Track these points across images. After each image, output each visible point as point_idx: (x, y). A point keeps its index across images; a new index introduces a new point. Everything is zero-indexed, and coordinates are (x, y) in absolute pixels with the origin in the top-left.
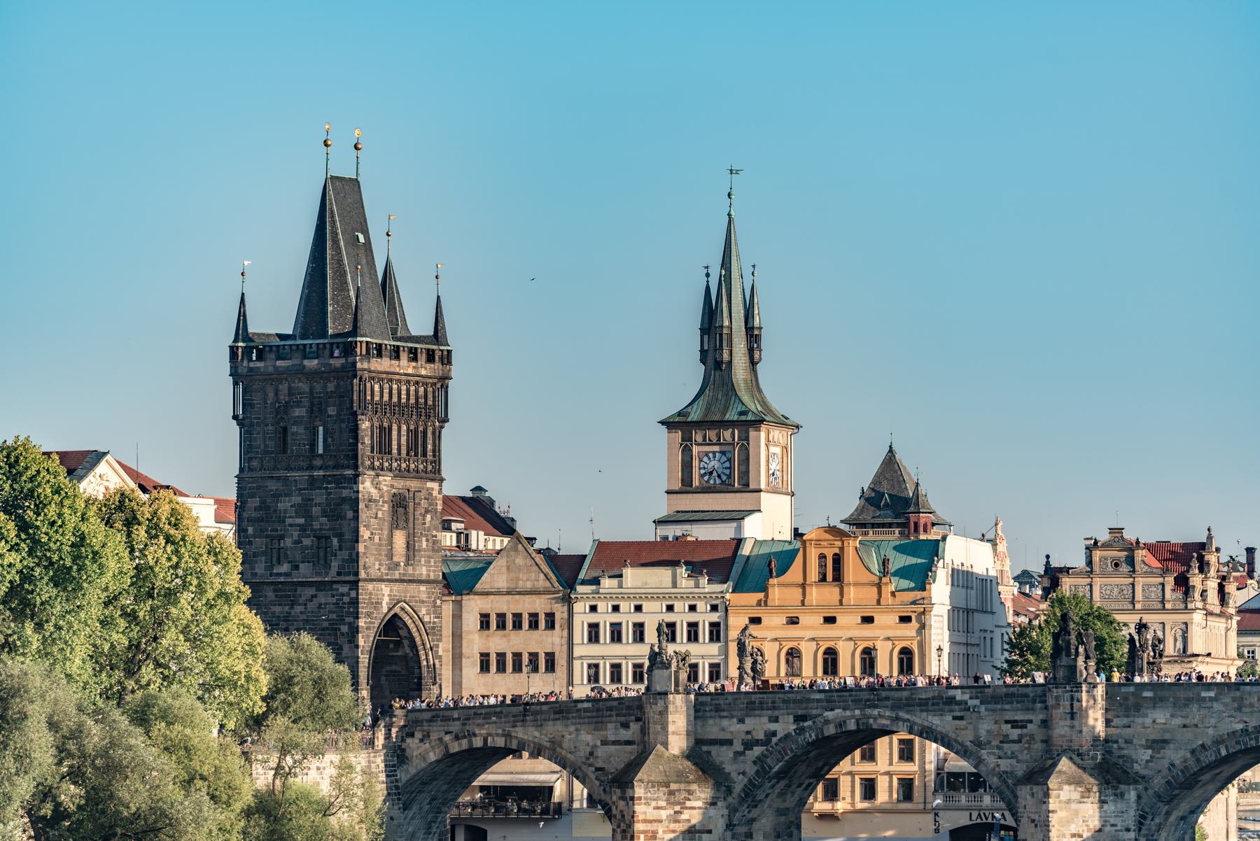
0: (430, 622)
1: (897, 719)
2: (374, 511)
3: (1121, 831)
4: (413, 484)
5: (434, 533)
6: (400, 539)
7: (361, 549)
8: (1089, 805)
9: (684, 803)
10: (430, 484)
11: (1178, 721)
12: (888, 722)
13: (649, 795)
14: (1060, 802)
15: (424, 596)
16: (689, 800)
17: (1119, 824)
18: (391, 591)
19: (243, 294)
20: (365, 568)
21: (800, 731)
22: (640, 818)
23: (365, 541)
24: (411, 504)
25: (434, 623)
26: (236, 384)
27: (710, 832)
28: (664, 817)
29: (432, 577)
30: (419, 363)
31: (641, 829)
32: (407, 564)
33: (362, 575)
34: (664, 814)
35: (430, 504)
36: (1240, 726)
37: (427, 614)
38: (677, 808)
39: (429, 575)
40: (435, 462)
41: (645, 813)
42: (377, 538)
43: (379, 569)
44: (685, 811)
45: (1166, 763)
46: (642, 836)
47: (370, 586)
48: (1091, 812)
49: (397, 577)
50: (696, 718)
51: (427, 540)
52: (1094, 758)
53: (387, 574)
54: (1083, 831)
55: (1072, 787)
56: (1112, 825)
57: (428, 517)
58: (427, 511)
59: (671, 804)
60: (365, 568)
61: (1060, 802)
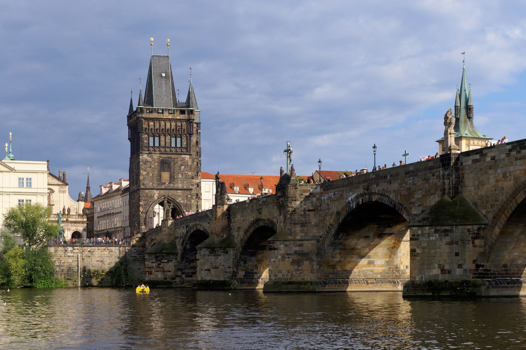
0: (184, 203)
1: (201, 225)
2: (149, 165)
3: (227, 268)
4: (173, 156)
5: (187, 172)
6: (166, 176)
7: (141, 178)
8: (213, 257)
9: (161, 261)
10: (183, 156)
11: (242, 219)
12: (199, 226)
13: (150, 258)
14: (201, 255)
15: (180, 194)
16: (163, 259)
17: (226, 265)
18: (159, 192)
19: (131, 99)
20: (143, 184)
21: (187, 232)
22: (147, 266)
23: (143, 175)
24: (172, 163)
25: (186, 203)
26: (129, 128)
27: (170, 271)
28: (155, 266)
29: (185, 187)
30: (176, 115)
31: (147, 270)
32: (170, 183)
33: (142, 187)
34: (154, 265)
35: (183, 163)
36: (252, 219)
37: (182, 200)
38: (159, 263)
39: (183, 187)
40: (187, 148)
41: (148, 264)
42: (151, 175)
43: (152, 185)
44: (162, 264)
45: (240, 237)
46: (147, 273)
47: (147, 191)
48: (214, 260)
49: (163, 187)
50: (175, 229)
51: (182, 175)
52: (222, 236)
53: (156, 187)
54: (210, 268)
55: (206, 249)
56: (223, 266)
57: (183, 167)
58: (182, 165)
59: (157, 261)
60: (143, 184)
61: (201, 255)
